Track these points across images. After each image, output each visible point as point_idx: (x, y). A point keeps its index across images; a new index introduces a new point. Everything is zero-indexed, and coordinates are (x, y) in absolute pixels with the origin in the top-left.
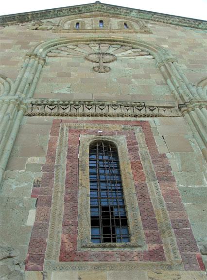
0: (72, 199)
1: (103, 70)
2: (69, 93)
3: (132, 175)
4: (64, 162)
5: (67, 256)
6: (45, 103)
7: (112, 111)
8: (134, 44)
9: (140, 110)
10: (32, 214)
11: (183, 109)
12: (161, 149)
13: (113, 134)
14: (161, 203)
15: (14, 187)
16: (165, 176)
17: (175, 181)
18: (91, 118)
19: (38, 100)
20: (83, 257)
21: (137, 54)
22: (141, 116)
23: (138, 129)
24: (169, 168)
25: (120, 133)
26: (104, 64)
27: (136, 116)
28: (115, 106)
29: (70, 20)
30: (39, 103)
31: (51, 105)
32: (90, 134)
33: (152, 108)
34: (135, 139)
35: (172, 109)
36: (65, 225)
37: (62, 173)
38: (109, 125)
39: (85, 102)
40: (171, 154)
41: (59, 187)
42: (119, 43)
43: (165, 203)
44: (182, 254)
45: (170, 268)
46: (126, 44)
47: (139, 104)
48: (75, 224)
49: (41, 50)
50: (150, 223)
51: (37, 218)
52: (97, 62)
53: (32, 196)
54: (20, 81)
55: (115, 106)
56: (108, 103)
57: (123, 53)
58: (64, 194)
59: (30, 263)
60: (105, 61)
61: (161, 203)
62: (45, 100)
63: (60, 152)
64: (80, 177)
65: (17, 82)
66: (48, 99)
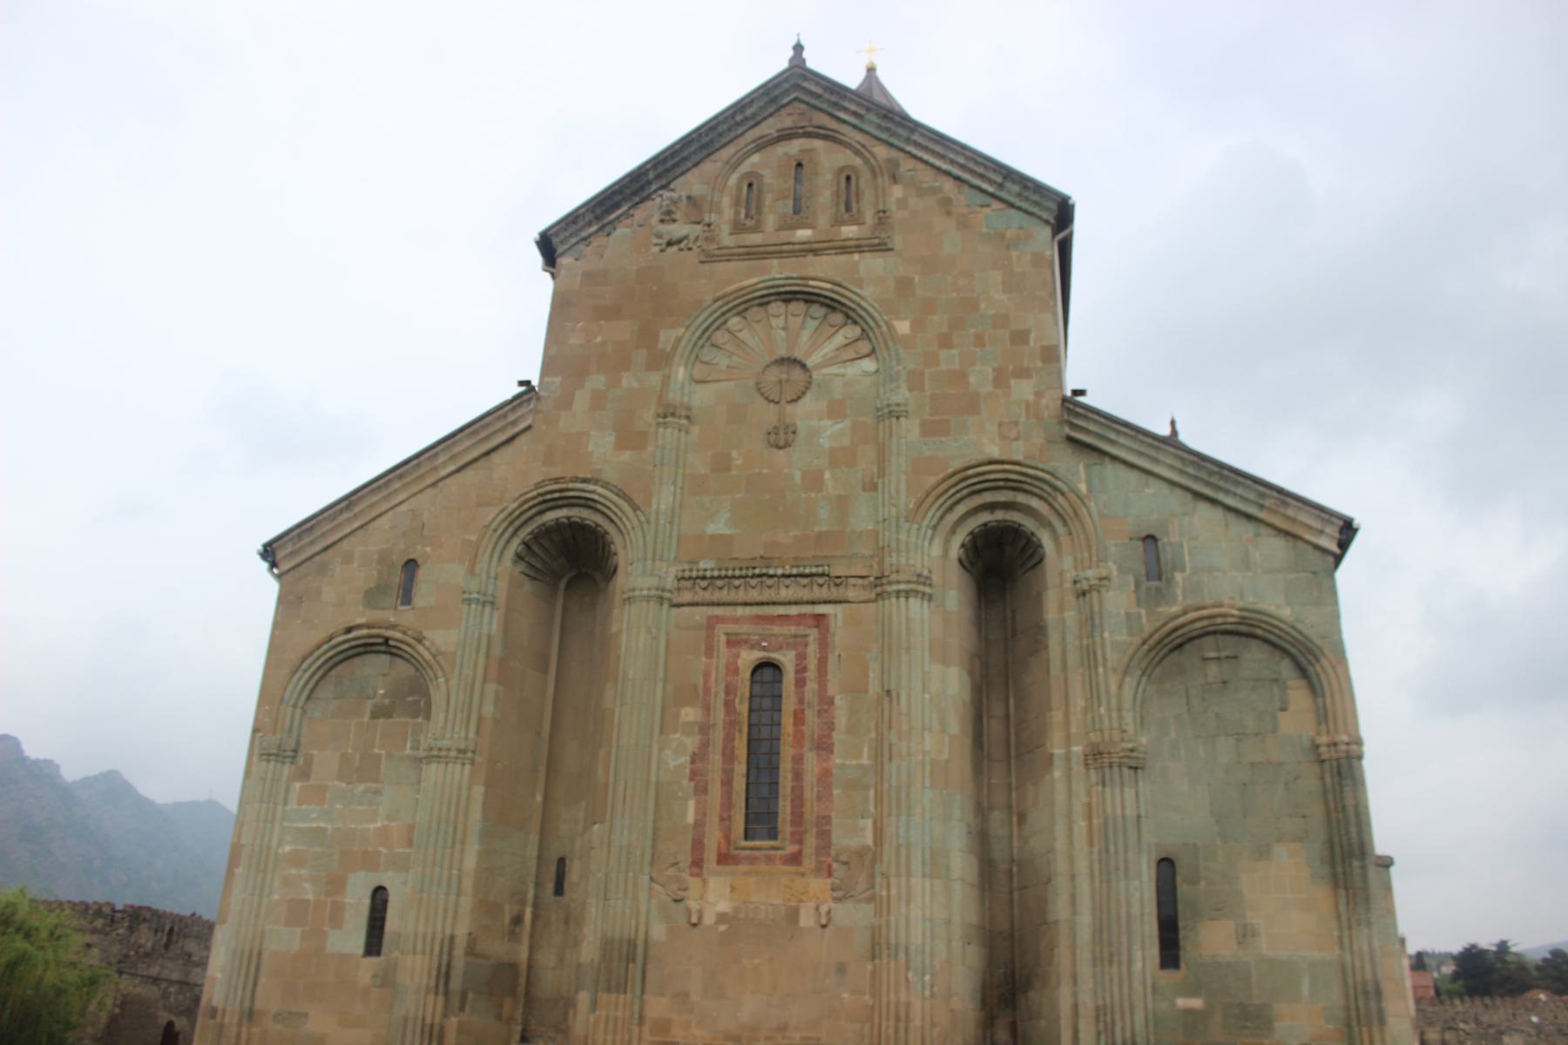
0: (727, 782)
1: (782, 443)
2: (728, 532)
3: (791, 738)
4: (719, 715)
5: (724, 859)
6: (694, 574)
7: (785, 594)
8: (850, 308)
9: (821, 586)
10: (691, 804)
11: (879, 590)
12: (832, 689)
13: (780, 648)
14: (812, 789)
15: (672, 764)
16: (824, 746)
17: (832, 752)
18: (756, 610)
19: (686, 567)
20: (735, 860)
21: (850, 354)
22: (820, 603)
23: (813, 634)
24: (831, 727)
25: (790, 646)
26: (789, 408)
27: (813, 603)
28: (789, 576)
29: (733, 172)
30: (687, 574)
31: (704, 578)
32: (752, 647)
33: (838, 581)
34: (805, 659)
35: (866, 582)
36: (722, 819)
37: (718, 736)
38: (776, 629)
39: (747, 568)
40: (841, 698)
41: (716, 758)
42: (822, 299)
43: (816, 789)
44: (817, 861)
45: (803, 875)
46: (835, 305)
47: (820, 570)
48: (730, 818)
49: (681, 370)
50: (798, 818)
51: (697, 813)
52: (777, 403)
53: (691, 779)
54: (657, 521)
55: (789, 576)
56: (780, 572)
57: (829, 348)
58: (720, 773)
59: (693, 868)
60: (789, 399)
61: (812, 789)
62: (695, 567)
63: (716, 697)
64: (737, 742)
65: (653, 525)
66: (697, 563)
